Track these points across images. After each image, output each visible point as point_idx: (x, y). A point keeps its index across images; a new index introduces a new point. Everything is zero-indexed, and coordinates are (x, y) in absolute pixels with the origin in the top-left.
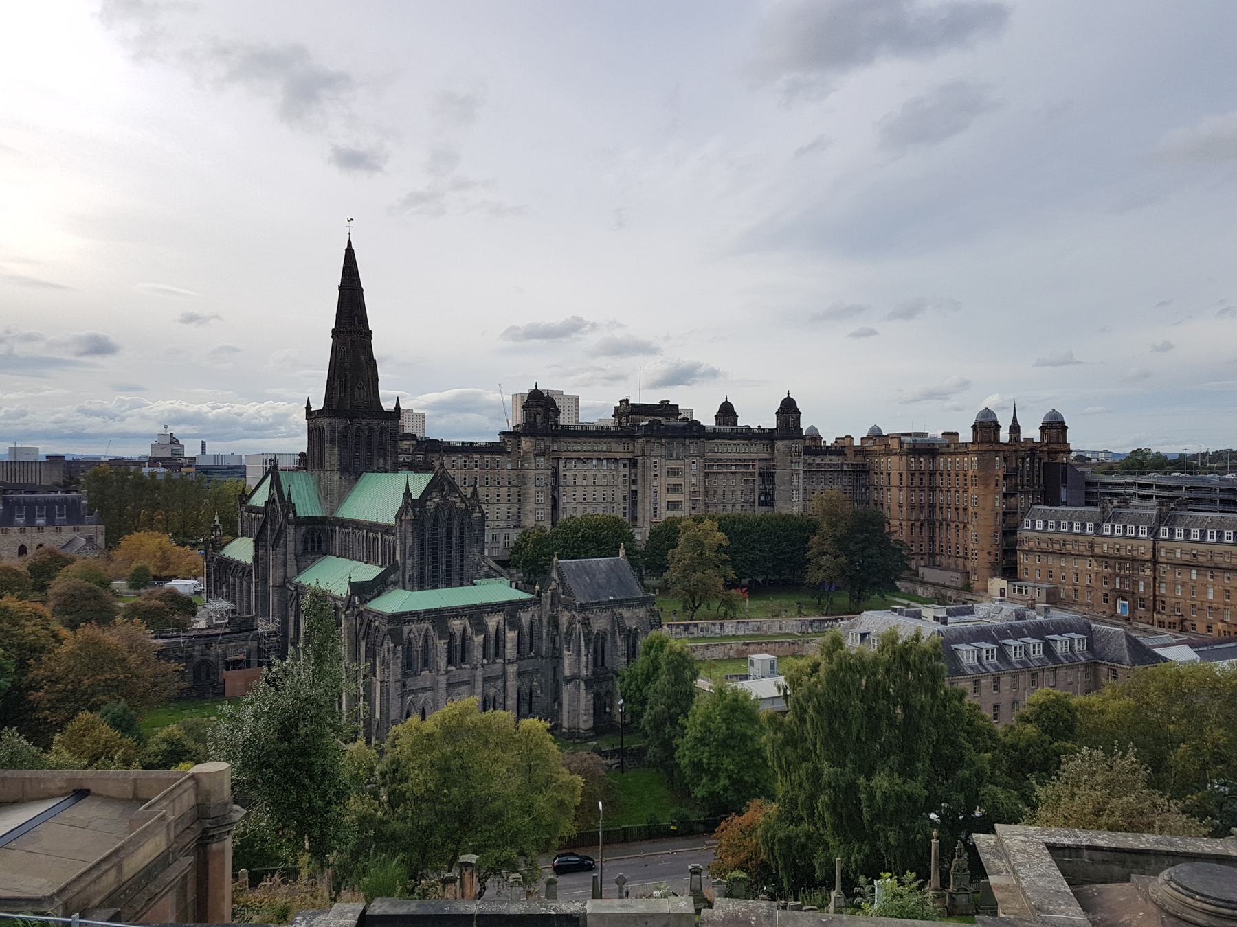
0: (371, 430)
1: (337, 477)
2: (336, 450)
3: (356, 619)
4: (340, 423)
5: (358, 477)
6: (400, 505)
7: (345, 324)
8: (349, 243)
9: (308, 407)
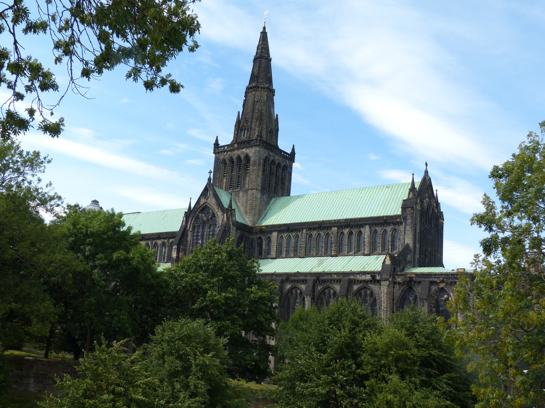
0: (279, 164)
1: (259, 196)
2: (261, 173)
3: (394, 287)
4: (264, 153)
5: (270, 199)
6: (405, 199)
7: (262, 82)
8: (264, 28)
9: (216, 144)
